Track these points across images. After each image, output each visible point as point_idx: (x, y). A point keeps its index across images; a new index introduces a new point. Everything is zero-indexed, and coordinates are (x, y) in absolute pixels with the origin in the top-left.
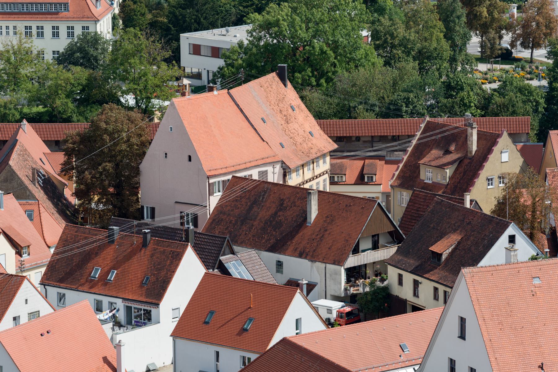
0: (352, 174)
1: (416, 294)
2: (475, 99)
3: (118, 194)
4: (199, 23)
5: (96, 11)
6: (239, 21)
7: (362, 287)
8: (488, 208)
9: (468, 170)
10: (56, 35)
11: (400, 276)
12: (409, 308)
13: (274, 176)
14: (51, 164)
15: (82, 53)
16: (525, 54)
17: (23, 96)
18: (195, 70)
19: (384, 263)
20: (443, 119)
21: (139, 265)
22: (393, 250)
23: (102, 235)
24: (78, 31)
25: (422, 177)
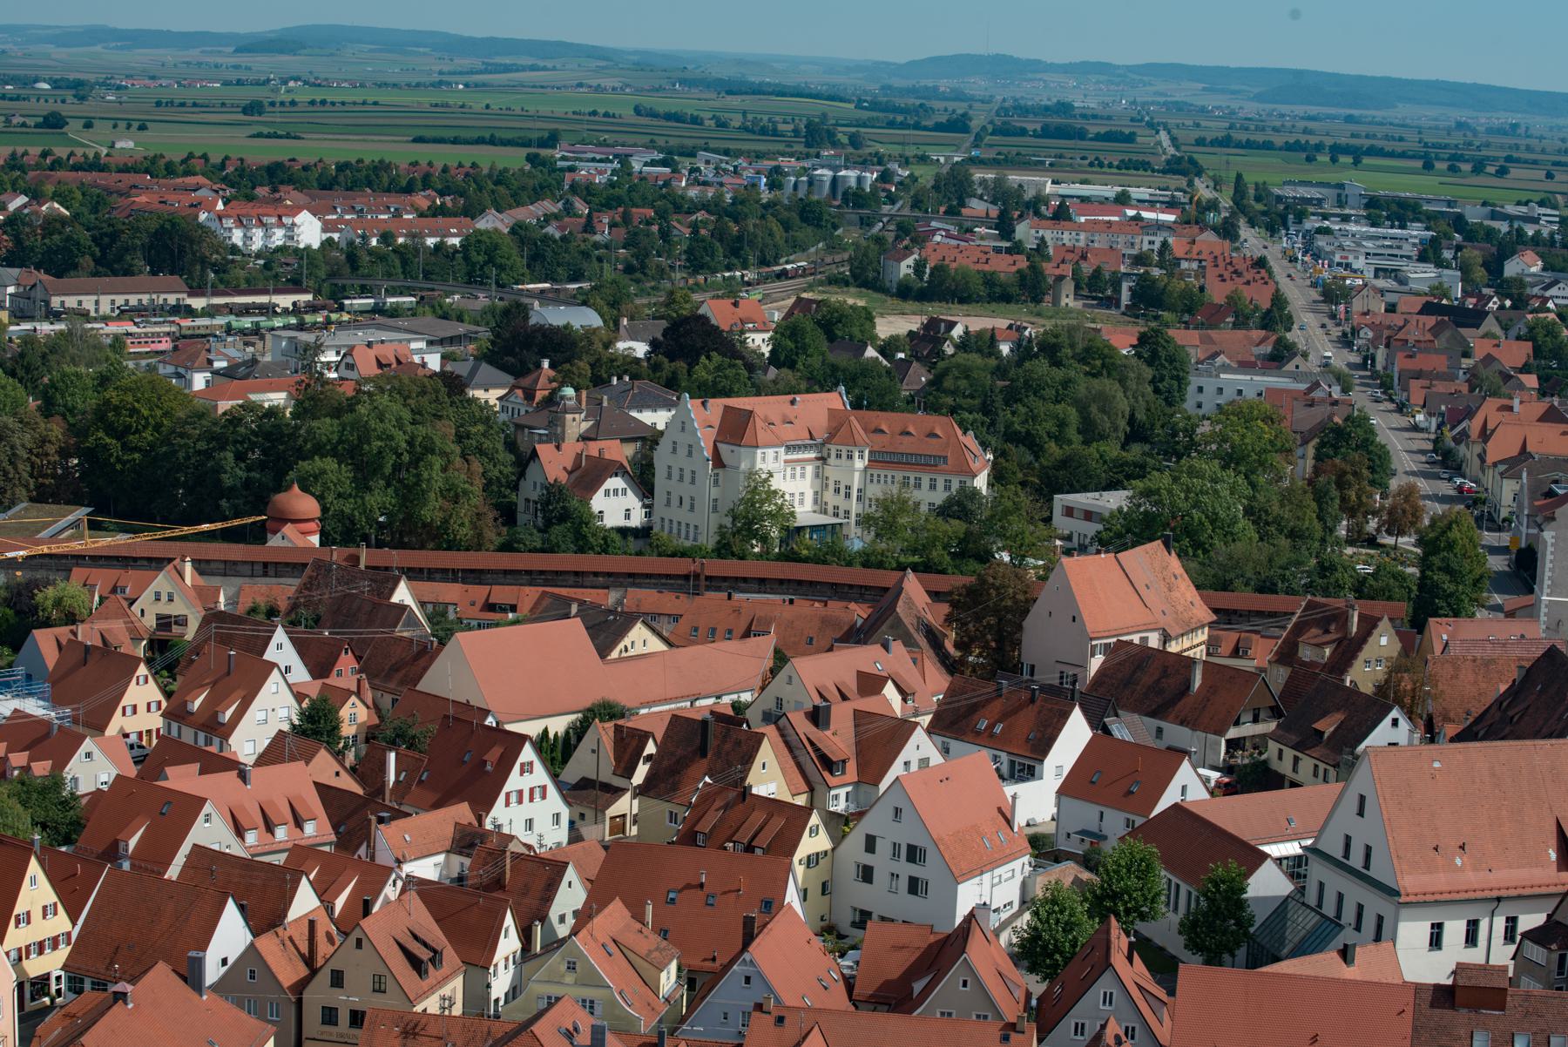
0: (1226, 648)
1: (1295, 770)
2: (1349, 583)
3: (999, 649)
4: (1071, 486)
5: (975, 466)
6: (1112, 486)
7: (1242, 759)
8: (1367, 688)
9: (1349, 650)
10: (933, 487)
11: (1281, 751)
12: (1287, 784)
13: (1154, 641)
14: (936, 615)
15: (959, 506)
16: (1389, 540)
17: (898, 545)
18: (1067, 532)
19: (1264, 737)
20: (1319, 599)
21: (1026, 720)
22: (1272, 726)
23: (990, 688)
24: (955, 486)
25: (1300, 654)
